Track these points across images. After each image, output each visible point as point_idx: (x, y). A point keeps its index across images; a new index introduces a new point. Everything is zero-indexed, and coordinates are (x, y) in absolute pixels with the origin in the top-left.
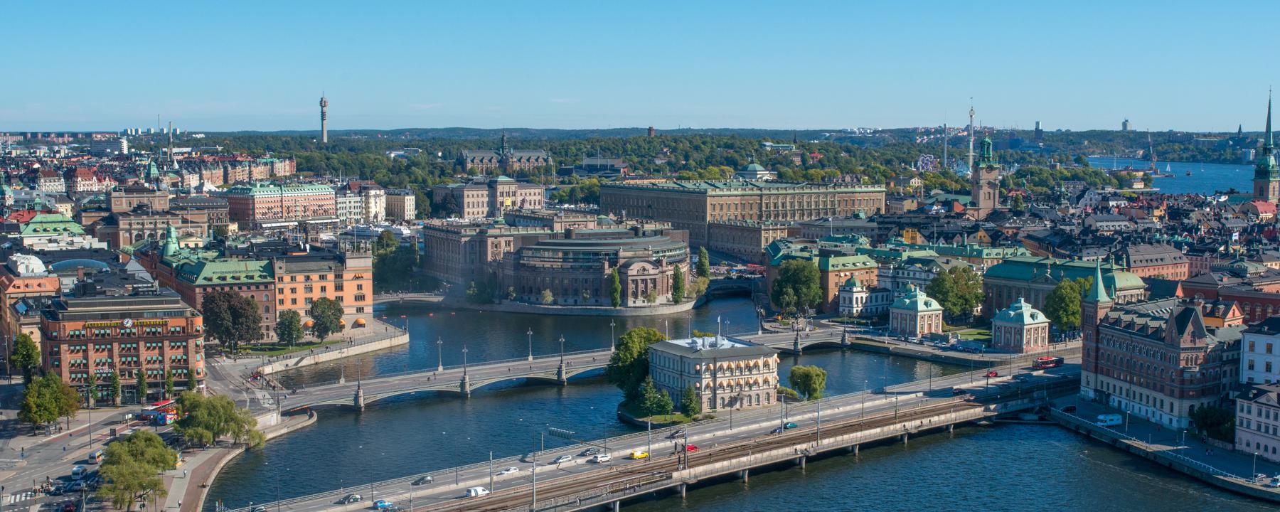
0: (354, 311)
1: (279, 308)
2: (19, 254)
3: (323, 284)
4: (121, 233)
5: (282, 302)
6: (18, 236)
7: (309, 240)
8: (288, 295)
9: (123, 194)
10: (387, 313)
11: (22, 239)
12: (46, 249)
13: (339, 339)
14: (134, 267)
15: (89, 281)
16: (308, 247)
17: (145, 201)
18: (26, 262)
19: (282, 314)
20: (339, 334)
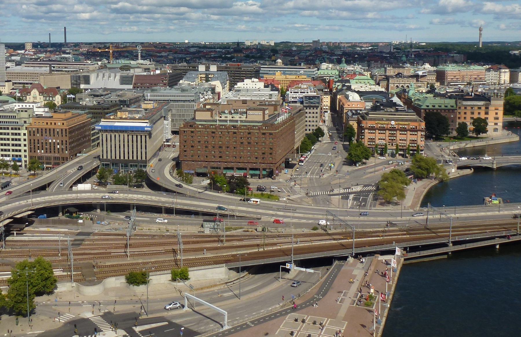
0: (493, 124)
1: (458, 121)
2: (350, 92)
3: (479, 111)
4: (390, 85)
5: (459, 118)
6: (349, 84)
7: (474, 91)
8: (463, 115)
9: (392, 68)
10: (509, 126)
11: (351, 86)
12: (360, 90)
13: (485, 136)
14: (395, 99)
15: (378, 104)
16: (473, 94)
17: (401, 71)
18: (352, 95)
19: (459, 124)
20: (485, 134)
